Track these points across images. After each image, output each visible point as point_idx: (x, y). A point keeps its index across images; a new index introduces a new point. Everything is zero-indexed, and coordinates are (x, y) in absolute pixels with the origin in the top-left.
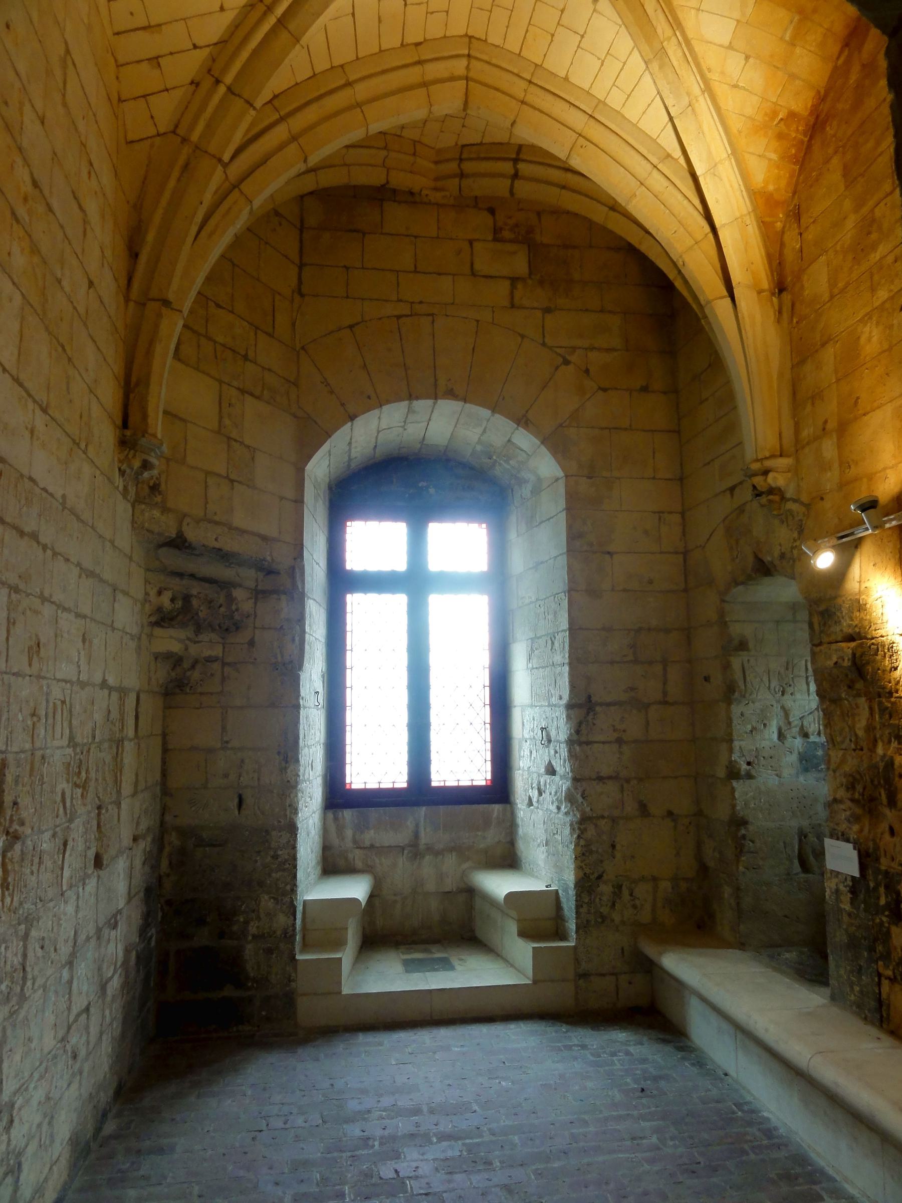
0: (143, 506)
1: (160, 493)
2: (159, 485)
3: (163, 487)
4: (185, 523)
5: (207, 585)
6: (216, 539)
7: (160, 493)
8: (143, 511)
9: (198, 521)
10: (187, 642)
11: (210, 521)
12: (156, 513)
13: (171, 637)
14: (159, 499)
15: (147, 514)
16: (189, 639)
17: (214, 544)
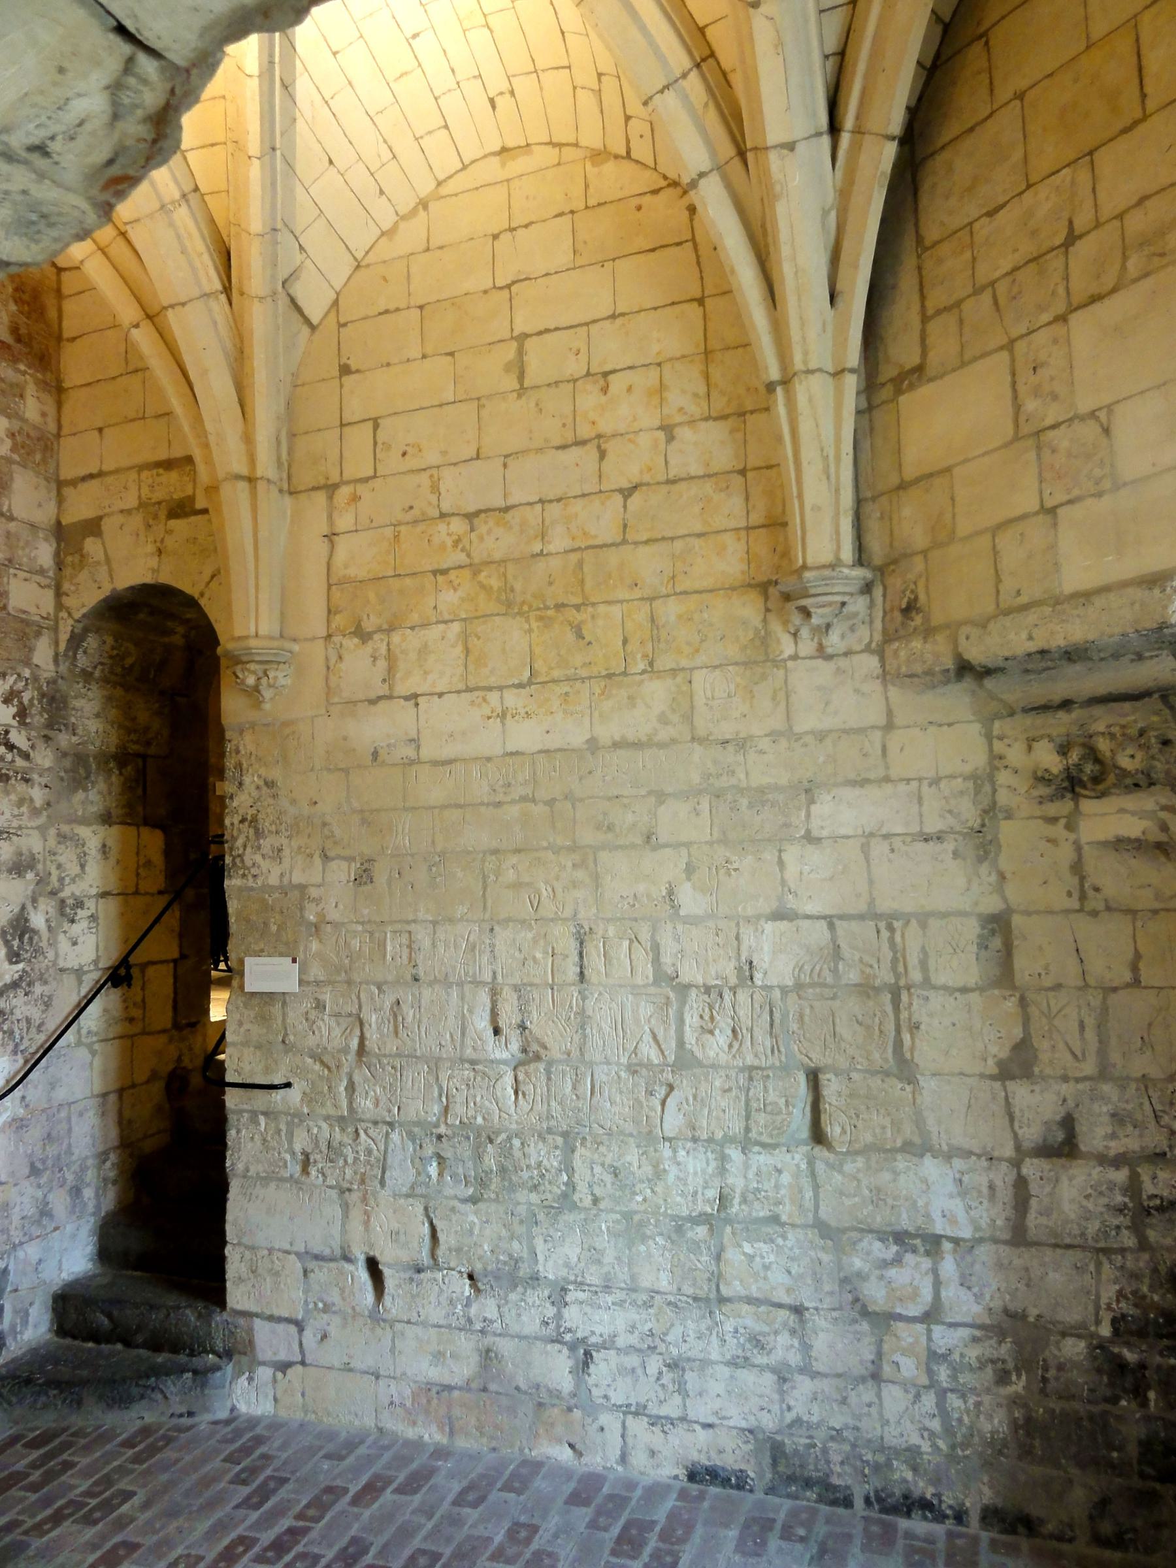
0: (896, 645)
1: (918, 611)
2: (916, 599)
3: (922, 597)
4: (962, 640)
5: (1127, 706)
6: (1030, 638)
7: (918, 611)
8: (896, 652)
9: (983, 624)
10: (1163, 815)
11: (1007, 612)
12: (917, 644)
13: (1122, 811)
14: (918, 620)
15: (902, 653)
16: (1164, 808)
17: (1032, 647)
